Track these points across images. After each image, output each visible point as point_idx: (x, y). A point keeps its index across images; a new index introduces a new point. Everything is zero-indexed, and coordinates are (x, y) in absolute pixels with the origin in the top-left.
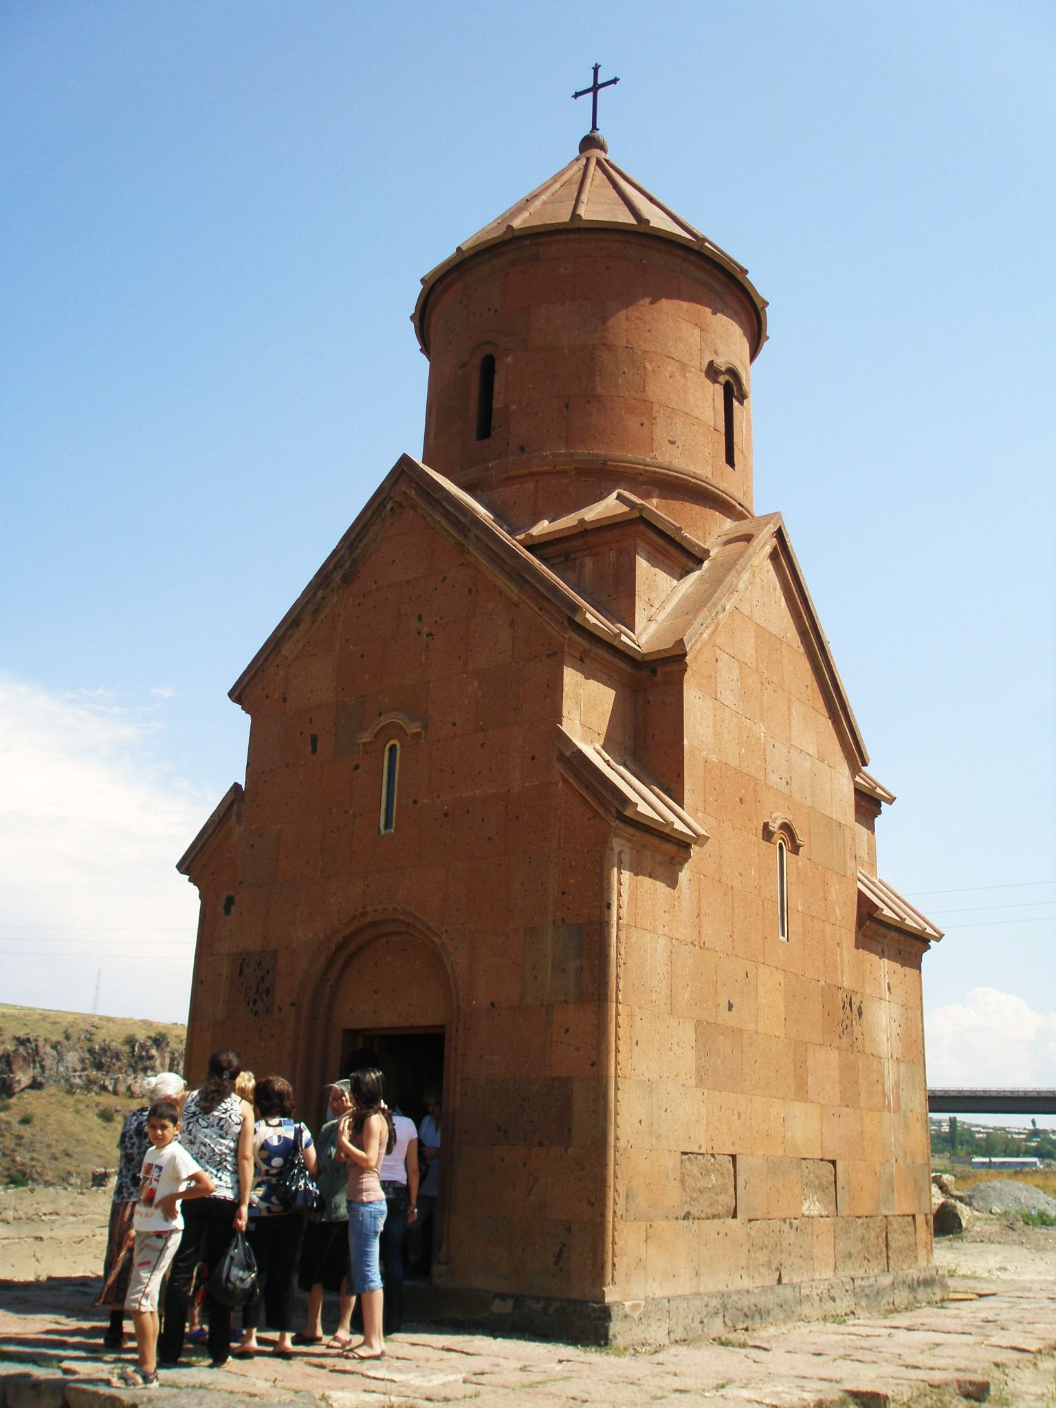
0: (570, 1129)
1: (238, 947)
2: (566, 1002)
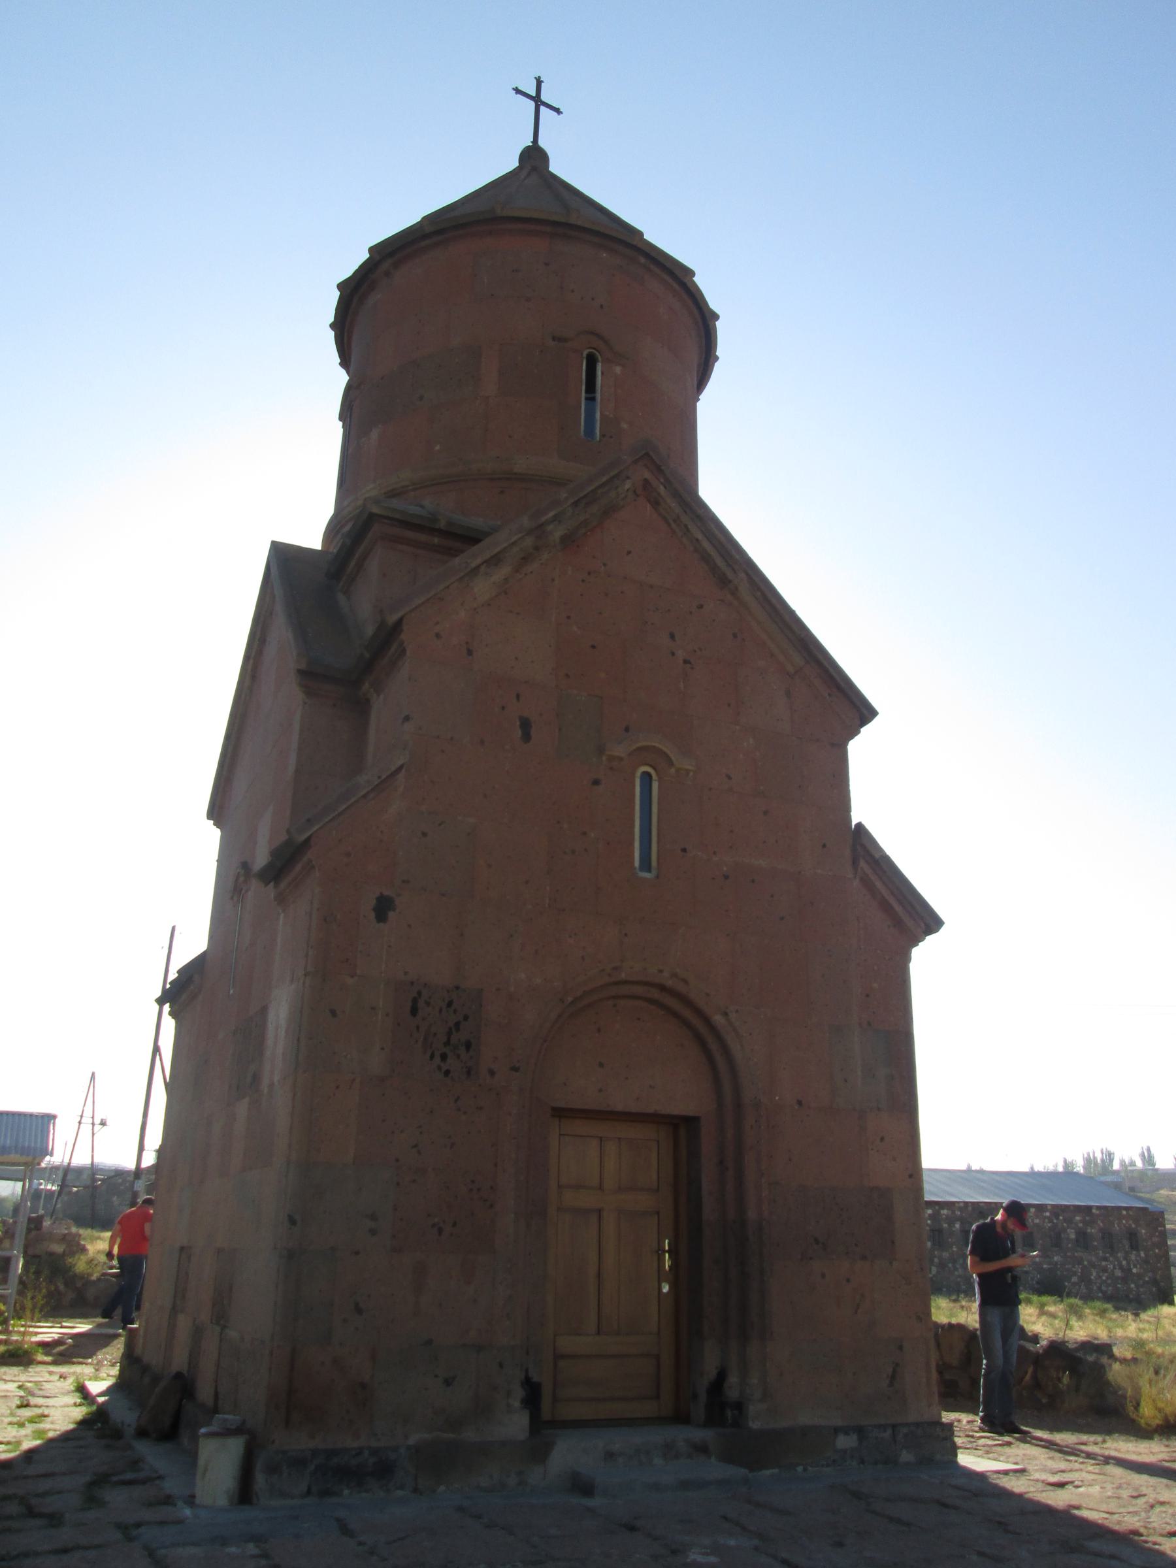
0: (893, 1242)
1: (406, 973)
2: (879, 1109)
